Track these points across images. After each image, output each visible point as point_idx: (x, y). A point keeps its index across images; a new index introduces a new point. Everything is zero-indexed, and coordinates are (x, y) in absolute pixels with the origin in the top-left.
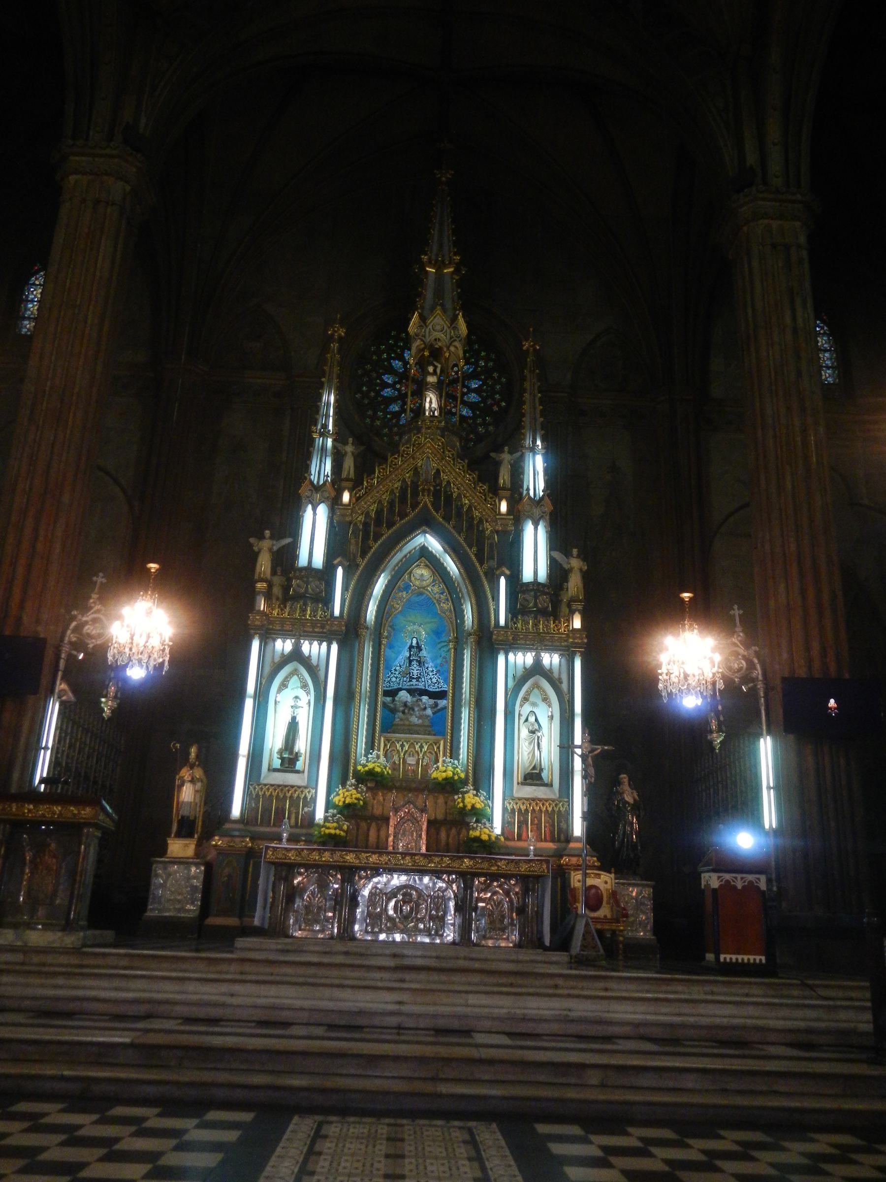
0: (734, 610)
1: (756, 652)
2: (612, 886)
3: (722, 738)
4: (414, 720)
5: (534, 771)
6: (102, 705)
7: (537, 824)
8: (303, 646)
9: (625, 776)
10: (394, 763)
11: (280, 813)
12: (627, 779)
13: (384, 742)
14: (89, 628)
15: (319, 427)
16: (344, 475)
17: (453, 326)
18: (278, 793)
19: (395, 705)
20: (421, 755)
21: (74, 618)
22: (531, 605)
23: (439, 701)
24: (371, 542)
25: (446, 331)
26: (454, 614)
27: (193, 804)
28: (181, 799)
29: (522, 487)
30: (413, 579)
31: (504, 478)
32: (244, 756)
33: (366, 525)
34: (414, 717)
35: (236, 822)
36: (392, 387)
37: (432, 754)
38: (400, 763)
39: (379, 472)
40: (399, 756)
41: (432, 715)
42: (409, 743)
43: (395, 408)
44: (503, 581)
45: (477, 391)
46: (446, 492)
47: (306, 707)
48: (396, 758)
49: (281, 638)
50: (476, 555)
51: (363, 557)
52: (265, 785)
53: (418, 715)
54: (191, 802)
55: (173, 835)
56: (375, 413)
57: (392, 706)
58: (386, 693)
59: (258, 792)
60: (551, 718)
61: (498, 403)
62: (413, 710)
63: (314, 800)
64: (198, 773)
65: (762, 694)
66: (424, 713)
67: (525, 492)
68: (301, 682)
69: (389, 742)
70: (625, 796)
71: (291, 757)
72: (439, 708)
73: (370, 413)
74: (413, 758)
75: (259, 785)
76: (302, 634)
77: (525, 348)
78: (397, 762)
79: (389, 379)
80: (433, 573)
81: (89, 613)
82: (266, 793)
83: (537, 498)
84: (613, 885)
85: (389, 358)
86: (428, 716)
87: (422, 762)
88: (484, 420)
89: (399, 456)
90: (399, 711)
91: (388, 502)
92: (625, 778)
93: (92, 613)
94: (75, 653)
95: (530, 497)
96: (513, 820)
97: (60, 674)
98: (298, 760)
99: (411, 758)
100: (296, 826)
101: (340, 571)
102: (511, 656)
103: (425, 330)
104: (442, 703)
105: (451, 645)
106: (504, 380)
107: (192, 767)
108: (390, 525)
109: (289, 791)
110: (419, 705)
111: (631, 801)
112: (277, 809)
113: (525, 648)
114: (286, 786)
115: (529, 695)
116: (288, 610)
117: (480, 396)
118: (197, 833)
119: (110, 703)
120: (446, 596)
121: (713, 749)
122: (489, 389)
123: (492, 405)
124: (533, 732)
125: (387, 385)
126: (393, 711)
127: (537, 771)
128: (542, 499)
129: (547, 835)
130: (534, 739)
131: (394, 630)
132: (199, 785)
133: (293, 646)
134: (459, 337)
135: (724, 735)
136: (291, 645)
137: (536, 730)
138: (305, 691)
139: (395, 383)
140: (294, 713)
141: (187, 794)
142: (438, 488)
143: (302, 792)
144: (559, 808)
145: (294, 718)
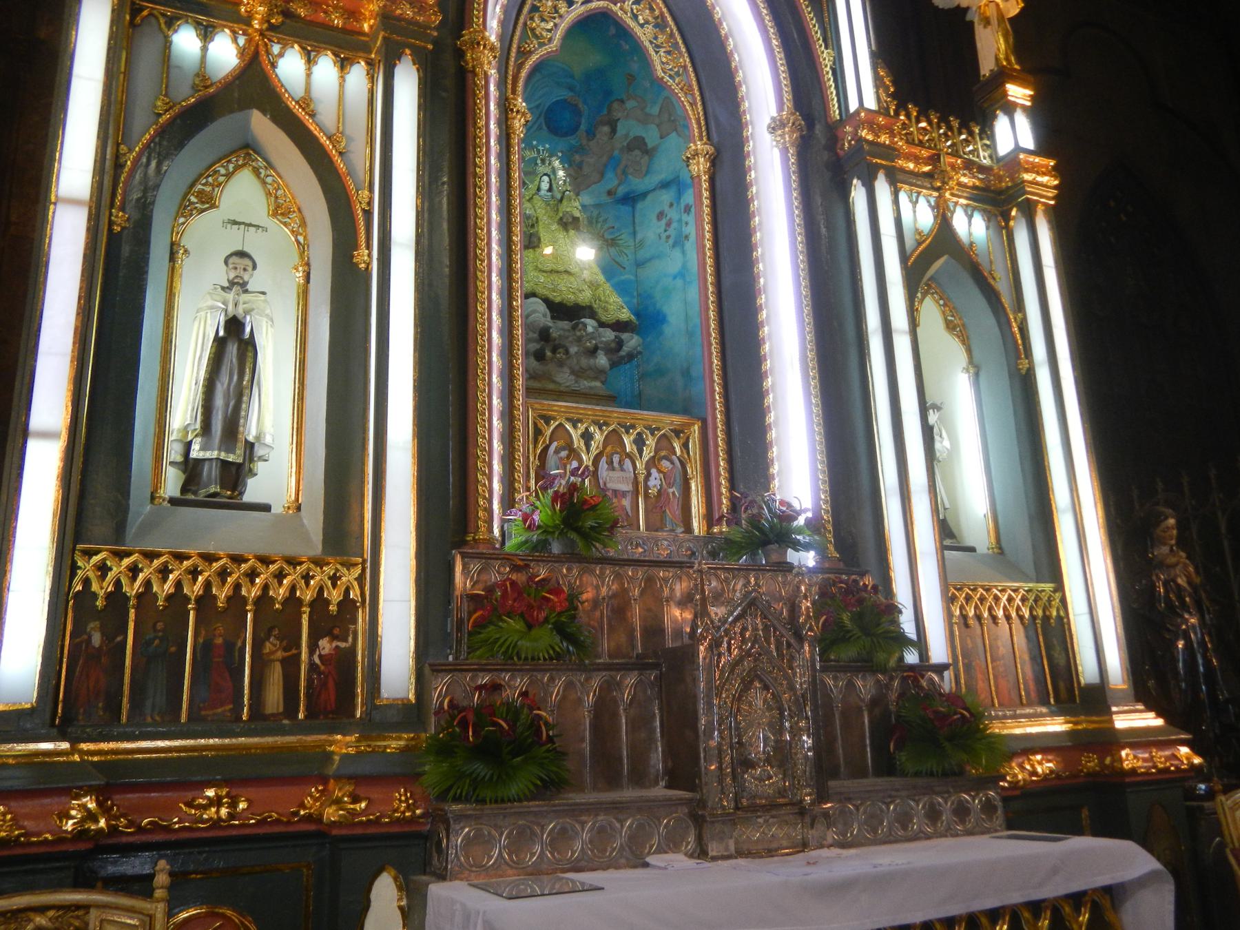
4: (565, 378)
13: (535, 424)
23: (625, 336)
34: (566, 370)
37: (672, 463)
42: (606, 430)
49: (197, 24)
53: (577, 368)
59: (118, 584)
62: (567, 352)
66: (592, 361)
68: (269, 194)
71: (231, 458)
74: (622, 474)
99: (617, 474)
104: (632, 341)
110: (579, 340)
112: (204, 651)
133: (242, 53)
138: (285, 224)
143: (307, 578)
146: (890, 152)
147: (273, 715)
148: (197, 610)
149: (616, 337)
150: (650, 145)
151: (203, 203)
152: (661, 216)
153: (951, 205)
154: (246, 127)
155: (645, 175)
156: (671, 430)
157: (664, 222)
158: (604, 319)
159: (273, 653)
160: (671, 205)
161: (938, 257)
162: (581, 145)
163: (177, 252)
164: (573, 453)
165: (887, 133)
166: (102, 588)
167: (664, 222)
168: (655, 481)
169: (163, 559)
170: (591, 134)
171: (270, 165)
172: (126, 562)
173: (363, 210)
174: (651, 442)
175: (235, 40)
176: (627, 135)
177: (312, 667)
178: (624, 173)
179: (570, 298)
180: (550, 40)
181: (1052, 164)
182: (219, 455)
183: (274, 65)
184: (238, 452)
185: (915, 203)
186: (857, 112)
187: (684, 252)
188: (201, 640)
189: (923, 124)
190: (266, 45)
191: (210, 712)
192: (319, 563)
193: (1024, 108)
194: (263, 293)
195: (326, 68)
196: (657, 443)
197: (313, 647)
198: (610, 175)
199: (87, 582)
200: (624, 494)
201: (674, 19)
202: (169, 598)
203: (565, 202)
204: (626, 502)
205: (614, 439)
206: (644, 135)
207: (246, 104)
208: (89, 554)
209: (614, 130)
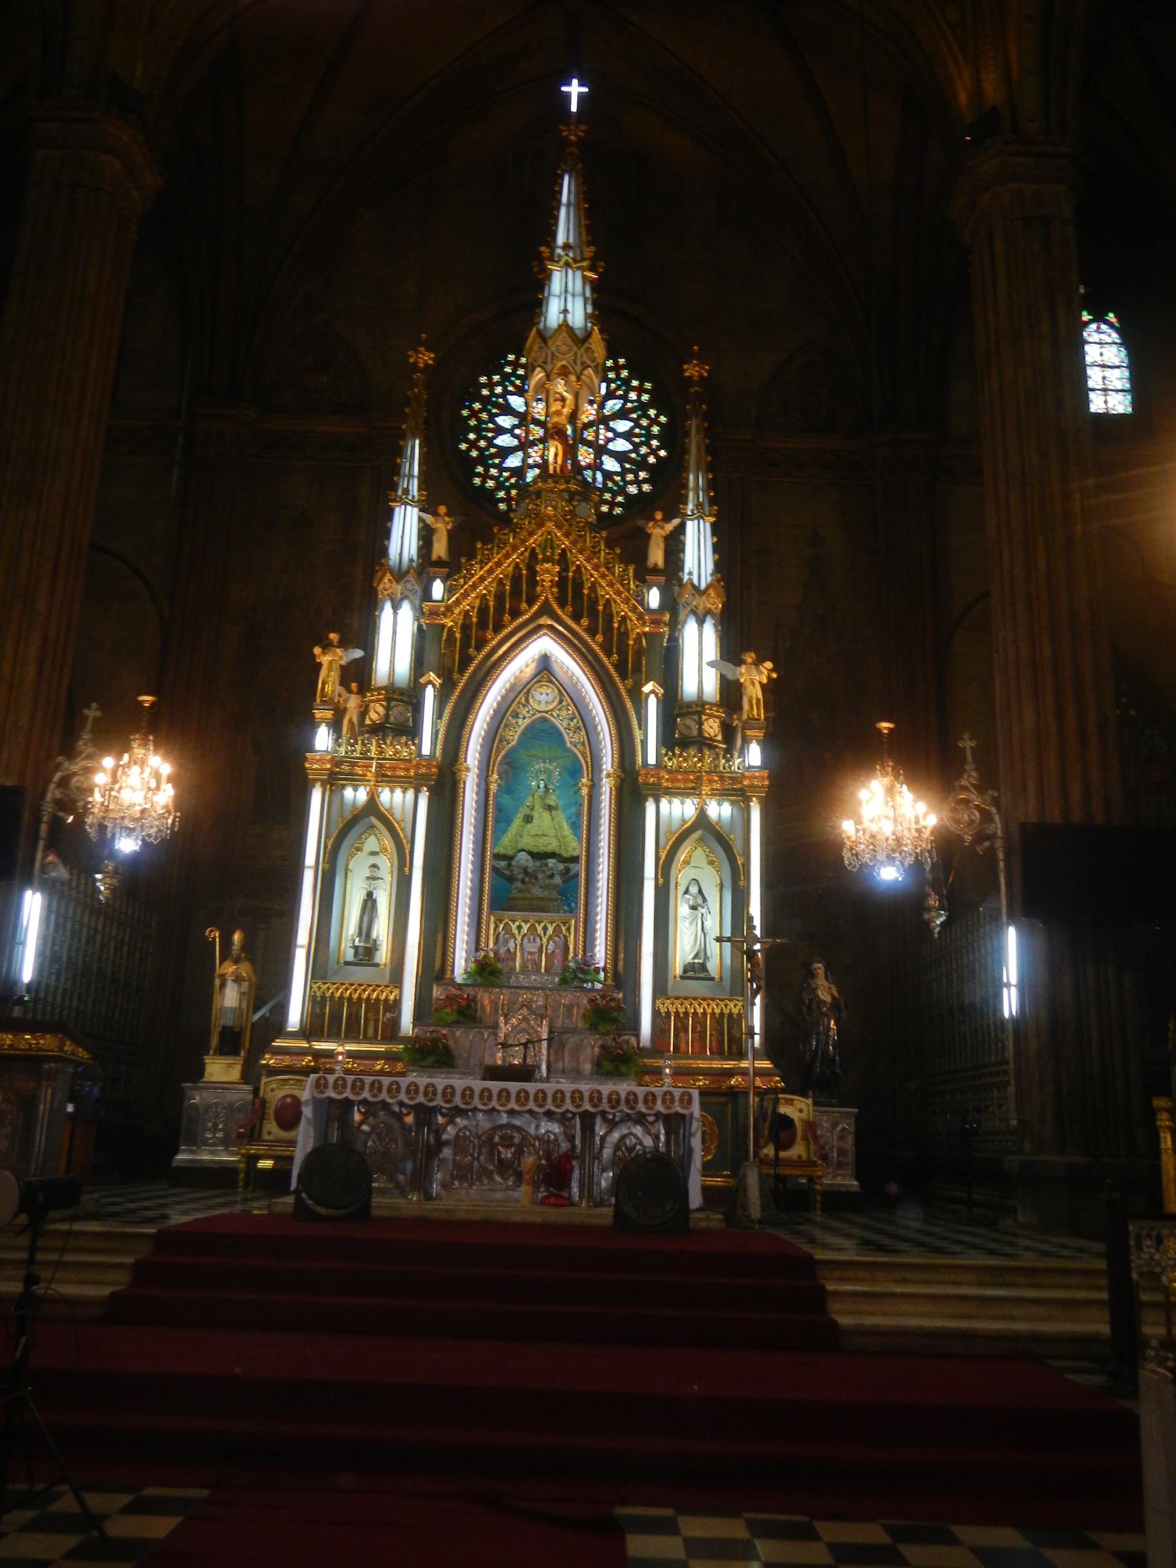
0: (964, 739)
1: (993, 797)
2: (809, 1114)
3: (944, 918)
4: (537, 891)
5: (696, 961)
6: (98, 884)
7: (699, 1032)
9: (819, 965)
10: (508, 950)
11: (353, 1019)
12: (823, 969)
14: (78, 781)
15: (400, 493)
16: (434, 557)
17: (587, 345)
19: (512, 871)
20: (545, 940)
21: (58, 767)
22: (695, 733)
23: (571, 866)
24: (471, 651)
25: (576, 354)
26: (588, 748)
27: (237, 1011)
28: (219, 1006)
29: (682, 569)
30: (531, 700)
31: (657, 556)
32: (302, 947)
33: (465, 628)
34: (537, 887)
35: (293, 1035)
36: (510, 431)
38: (516, 952)
39: (483, 555)
40: (515, 942)
41: (562, 884)
42: (528, 925)
43: (513, 461)
44: (652, 703)
45: (627, 436)
46: (574, 579)
47: (388, 878)
48: (511, 945)
49: (353, 785)
50: (616, 667)
51: (462, 670)
54: (235, 1008)
55: (211, 1052)
56: (487, 470)
57: (507, 873)
58: (497, 856)
59: (324, 993)
61: (654, 452)
62: (536, 878)
63: (397, 1004)
64: (245, 969)
65: (1001, 856)
67: (686, 578)
70: (819, 992)
71: (367, 946)
72: (571, 874)
73: (480, 469)
76: (380, 779)
77: (687, 374)
78: (512, 950)
79: (505, 421)
80: (559, 690)
81: (79, 759)
83: (703, 586)
84: (811, 1113)
85: (506, 393)
86: (556, 886)
87: (547, 950)
88: (637, 476)
89: (510, 531)
90: (517, 880)
91: (496, 596)
92: (819, 969)
93: (82, 760)
94: (61, 814)
95: (693, 585)
96: (667, 1026)
97: (41, 843)
98: (377, 950)
99: (532, 944)
101: (430, 694)
102: (664, 803)
103: (547, 355)
104: (574, 867)
106: (663, 419)
107: (237, 961)
108: (498, 628)
111: (828, 999)
112: (349, 1015)
113: (683, 793)
115: (690, 856)
116: (358, 747)
117: (632, 443)
118: (244, 1048)
119: (108, 880)
120: (578, 722)
121: (932, 933)
122: (643, 432)
123: (647, 455)
124: (694, 908)
125: (500, 431)
126: (511, 879)
127: (700, 961)
128: (709, 587)
129: (714, 1046)
130: (697, 917)
131: (512, 767)
132: (246, 984)
134: (593, 361)
135: (947, 913)
136: (365, 794)
137: (699, 905)
139: (515, 427)
140: (370, 886)
141: (230, 997)
142: (564, 574)
144: (730, 1010)
145: (370, 895)
149: (565, 867)
158: (565, 855)
161: (697, 830)
164: (513, 936)
168: (551, 946)
171: (380, 833)
172: (326, 986)
177: (383, 1023)
179: (542, 849)
180: (513, 740)
183: (379, 797)
192: (387, 986)
194: (382, 879)
197: (384, 1016)
199: (315, 992)
200: (533, 953)
202: (339, 997)
203: (548, 796)
204: (536, 957)
205: (532, 928)
207: (367, 816)
208: (316, 983)
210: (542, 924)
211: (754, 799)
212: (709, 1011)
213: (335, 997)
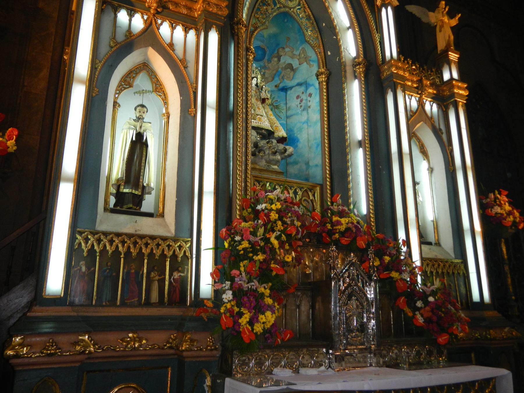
8: (162, 28)
18: (129, 248)
37: (308, 202)
52: (105, 234)
59: (93, 246)
60: (431, 170)
69: (259, 182)
75: (94, 234)
82: (108, 248)
100: (161, 303)
105: (323, 78)
109: (147, 245)
112: (127, 275)
114: (142, 237)
140: (141, 127)
145: (139, 136)
146: (403, 78)
147: (154, 303)
148: (125, 258)
150: (294, 68)
151: (127, 85)
152: (298, 97)
153: (425, 101)
154: (146, 54)
155: (292, 80)
156: (308, 188)
157: (299, 100)
159: (154, 277)
160: (303, 93)
161: (419, 122)
162: (265, 65)
163: (116, 105)
165: (402, 70)
166: (86, 247)
167: (299, 100)
169: (111, 236)
170: (269, 61)
173: (193, 92)
174: (300, 193)
175: (143, 17)
176: (285, 62)
177: (170, 283)
178: (283, 78)
181: (465, 86)
182: (132, 191)
184: (139, 190)
185: (411, 99)
186: (390, 61)
187: (308, 113)
188: (125, 271)
189: (414, 67)
190: (155, 20)
191: (129, 301)
193: (455, 62)
195: (179, 31)
196: (302, 194)
197: (171, 275)
198: (276, 79)
199: (80, 244)
201: (314, 17)
206: (292, 63)
207: (146, 46)
209: (279, 60)
210: (293, 189)
211: (460, 103)
212: (445, 271)
213: (108, 251)
